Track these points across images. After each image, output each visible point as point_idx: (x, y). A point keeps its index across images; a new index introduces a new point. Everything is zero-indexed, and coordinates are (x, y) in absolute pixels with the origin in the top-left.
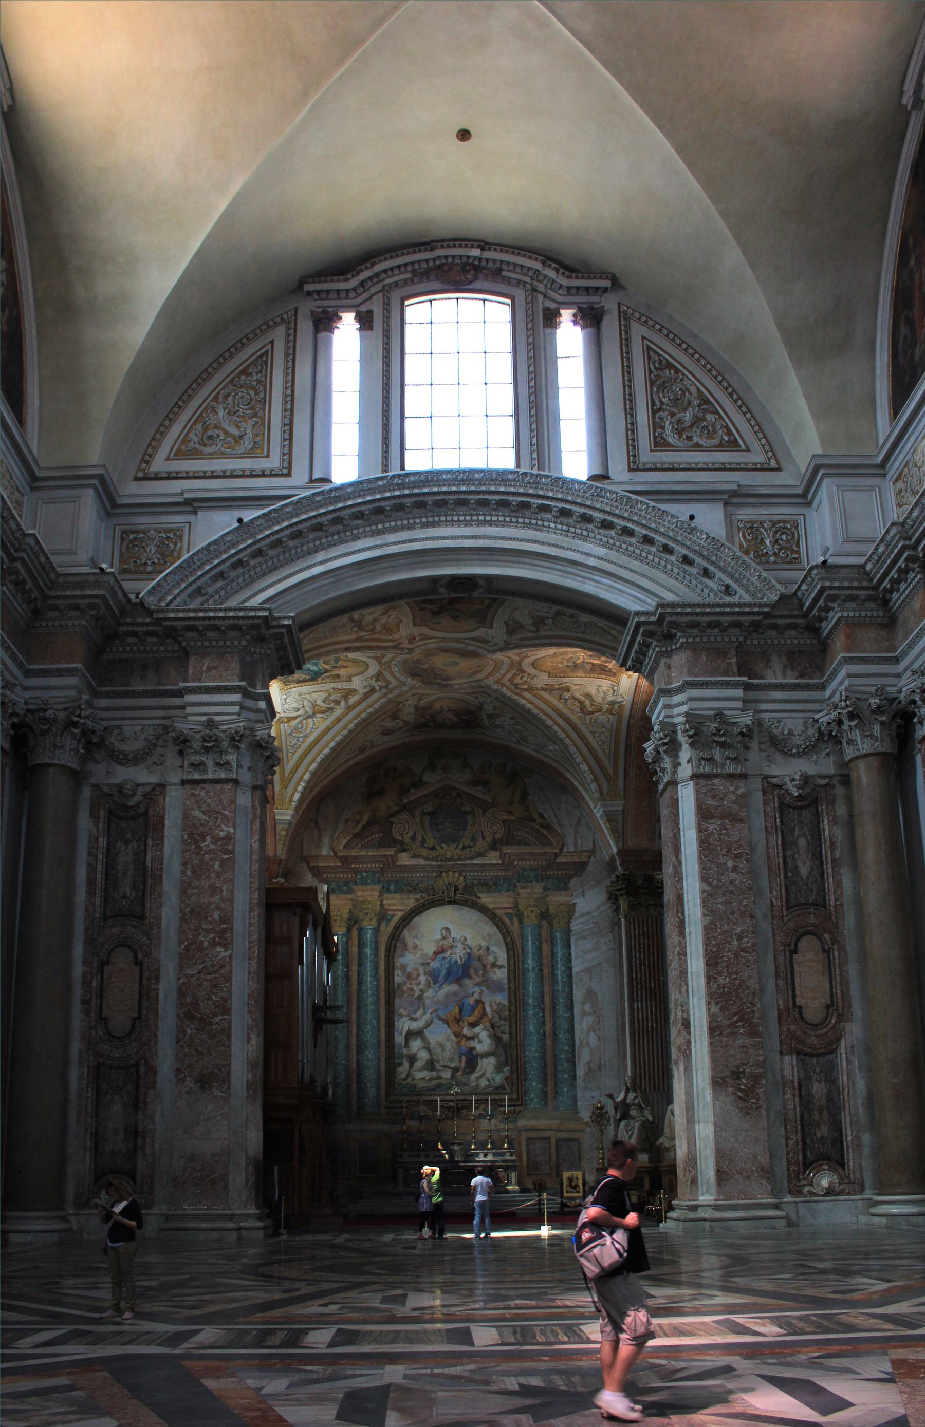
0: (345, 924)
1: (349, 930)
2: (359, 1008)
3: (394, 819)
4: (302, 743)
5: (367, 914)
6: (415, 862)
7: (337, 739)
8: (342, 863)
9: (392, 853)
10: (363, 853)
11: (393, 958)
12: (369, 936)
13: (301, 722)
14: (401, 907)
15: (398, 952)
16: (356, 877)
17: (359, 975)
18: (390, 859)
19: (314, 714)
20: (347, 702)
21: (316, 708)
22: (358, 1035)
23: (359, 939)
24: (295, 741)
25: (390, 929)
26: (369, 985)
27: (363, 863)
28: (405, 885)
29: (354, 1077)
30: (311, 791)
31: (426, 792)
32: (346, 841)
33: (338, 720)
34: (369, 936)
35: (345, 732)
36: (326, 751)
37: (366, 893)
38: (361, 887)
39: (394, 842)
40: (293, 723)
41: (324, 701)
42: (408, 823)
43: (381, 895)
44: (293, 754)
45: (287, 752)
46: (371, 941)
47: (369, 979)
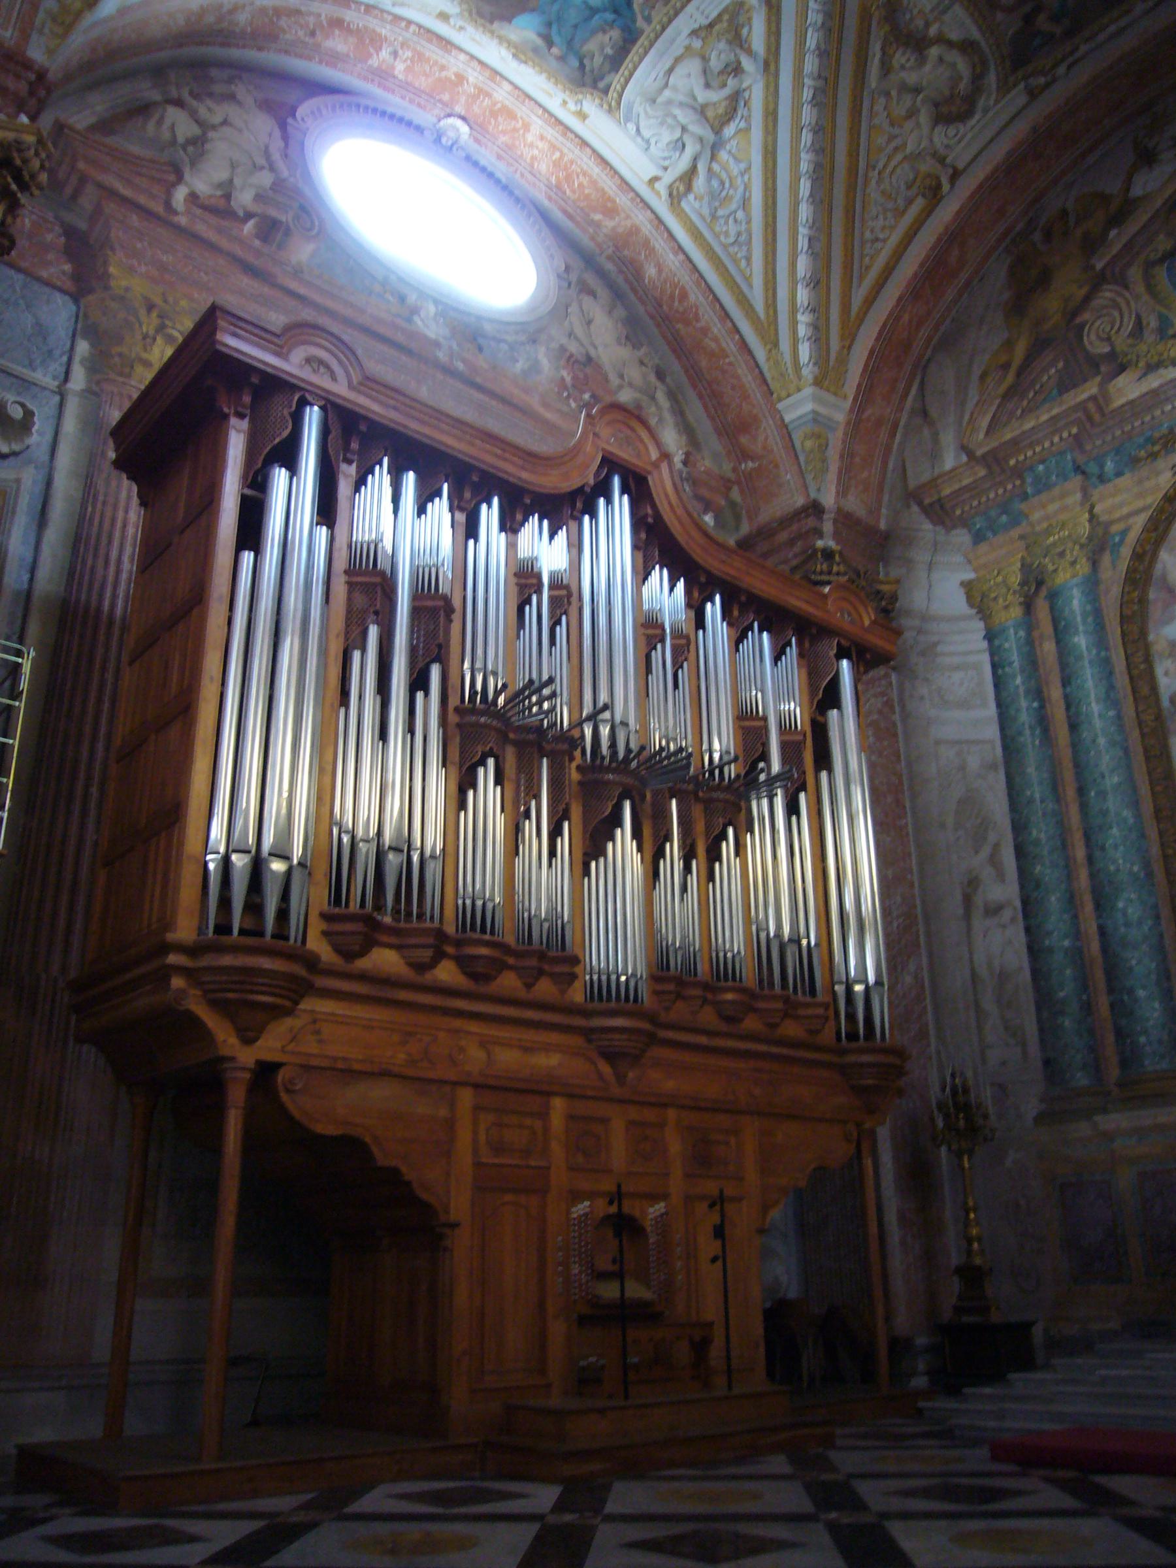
0: (1015, 600)
1: (1028, 606)
2: (1081, 791)
3: (1086, 316)
4: (749, 222)
5: (1062, 554)
6: (1154, 382)
7: (804, 166)
8: (989, 467)
9: (1094, 390)
10: (1029, 425)
11: (1143, 633)
12: (1076, 603)
13: (710, 170)
14: (1140, 504)
15: (1155, 612)
16: (1023, 482)
17: (1068, 708)
18: (1091, 406)
19: (718, 131)
20: (749, 52)
21: (710, 114)
22: (1090, 860)
23: (1055, 622)
24: (732, 229)
25: (1123, 566)
26: (1098, 724)
27: (1031, 446)
28: (1141, 447)
29: (1099, 975)
30: (849, 336)
31: (1145, 218)
32: (988, 417)
33: (771, 115)
34: (1076, 603)
35: (807, 137)
36: (805, 212)
37: (1052, 508)
38: (1035, 501)
39: (1094, 363)
40: (700, 182)
41: (707, 85)
42: (1116, 306)
43: (1086, 495)
44: (748, 259)
45: (736, 262)
46: (1084, 615)
47: (1095, 708)
